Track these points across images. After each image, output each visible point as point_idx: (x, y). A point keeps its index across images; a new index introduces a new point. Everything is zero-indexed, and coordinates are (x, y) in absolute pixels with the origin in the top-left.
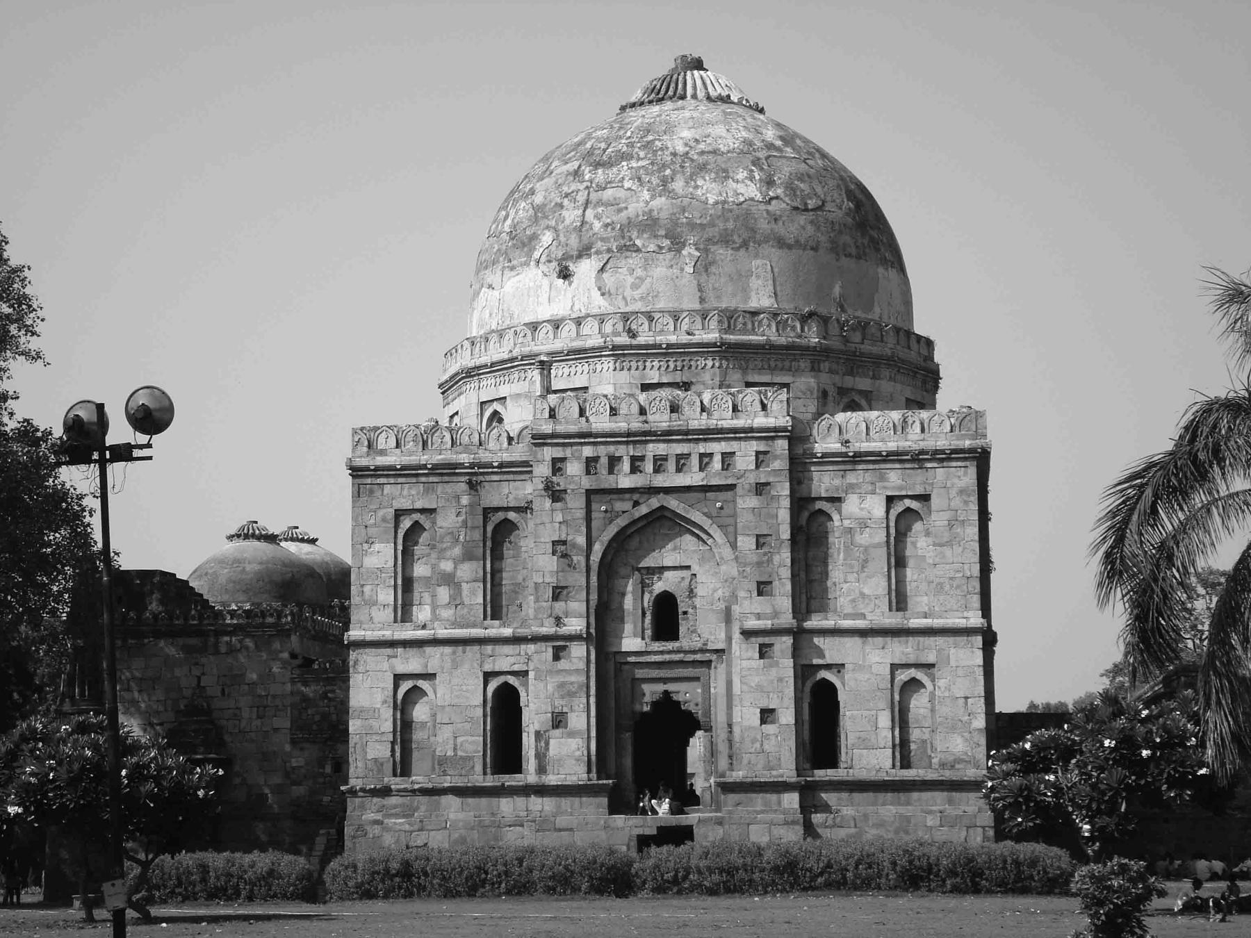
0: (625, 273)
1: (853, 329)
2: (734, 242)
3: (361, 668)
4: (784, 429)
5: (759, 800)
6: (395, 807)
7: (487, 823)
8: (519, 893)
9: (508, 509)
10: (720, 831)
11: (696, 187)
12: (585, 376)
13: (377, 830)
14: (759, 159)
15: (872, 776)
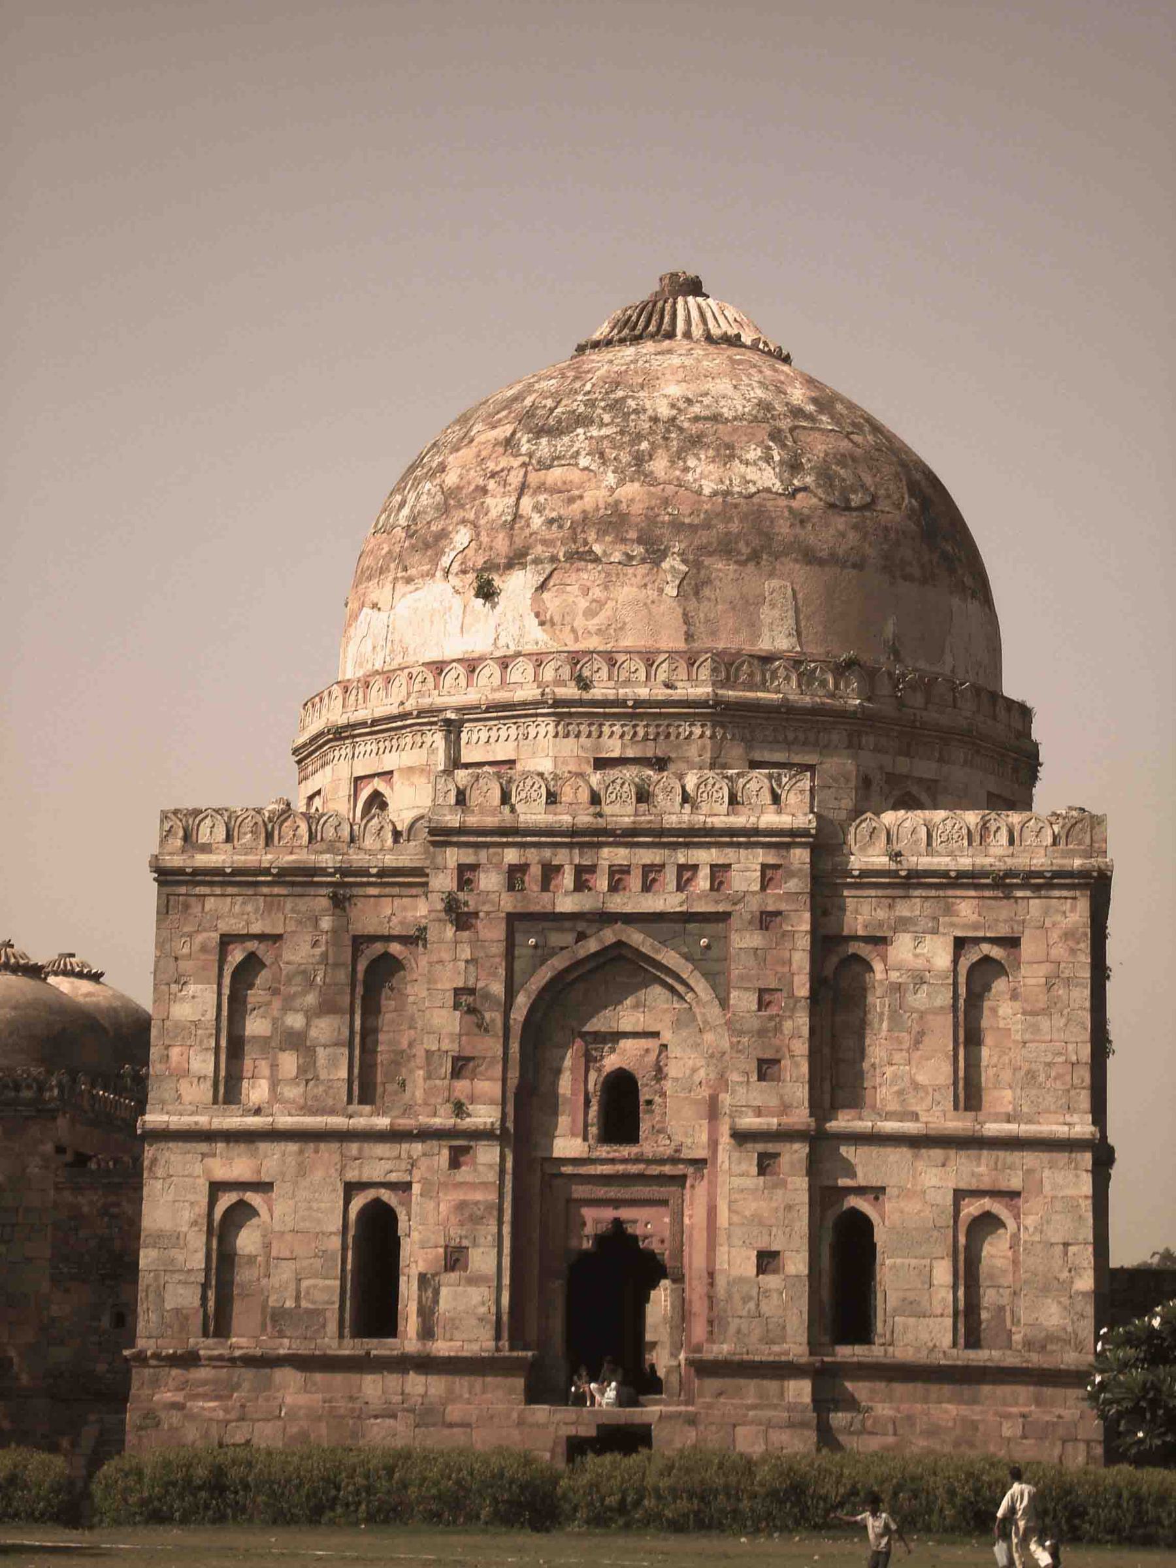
0: (576, 592)
1: (913, 687)
2: (739, 553)
3: (160, 1172)
4: (805, 833)
5: (751, 1388)
6: (205, 1383)
7: (342, 1411)
8: (386, 1521)
10: (691, 1435)
11: (686, 469)
12: (511, 744)
13: (175, 1418)
14: (780, 431)
15: (923, 1358)
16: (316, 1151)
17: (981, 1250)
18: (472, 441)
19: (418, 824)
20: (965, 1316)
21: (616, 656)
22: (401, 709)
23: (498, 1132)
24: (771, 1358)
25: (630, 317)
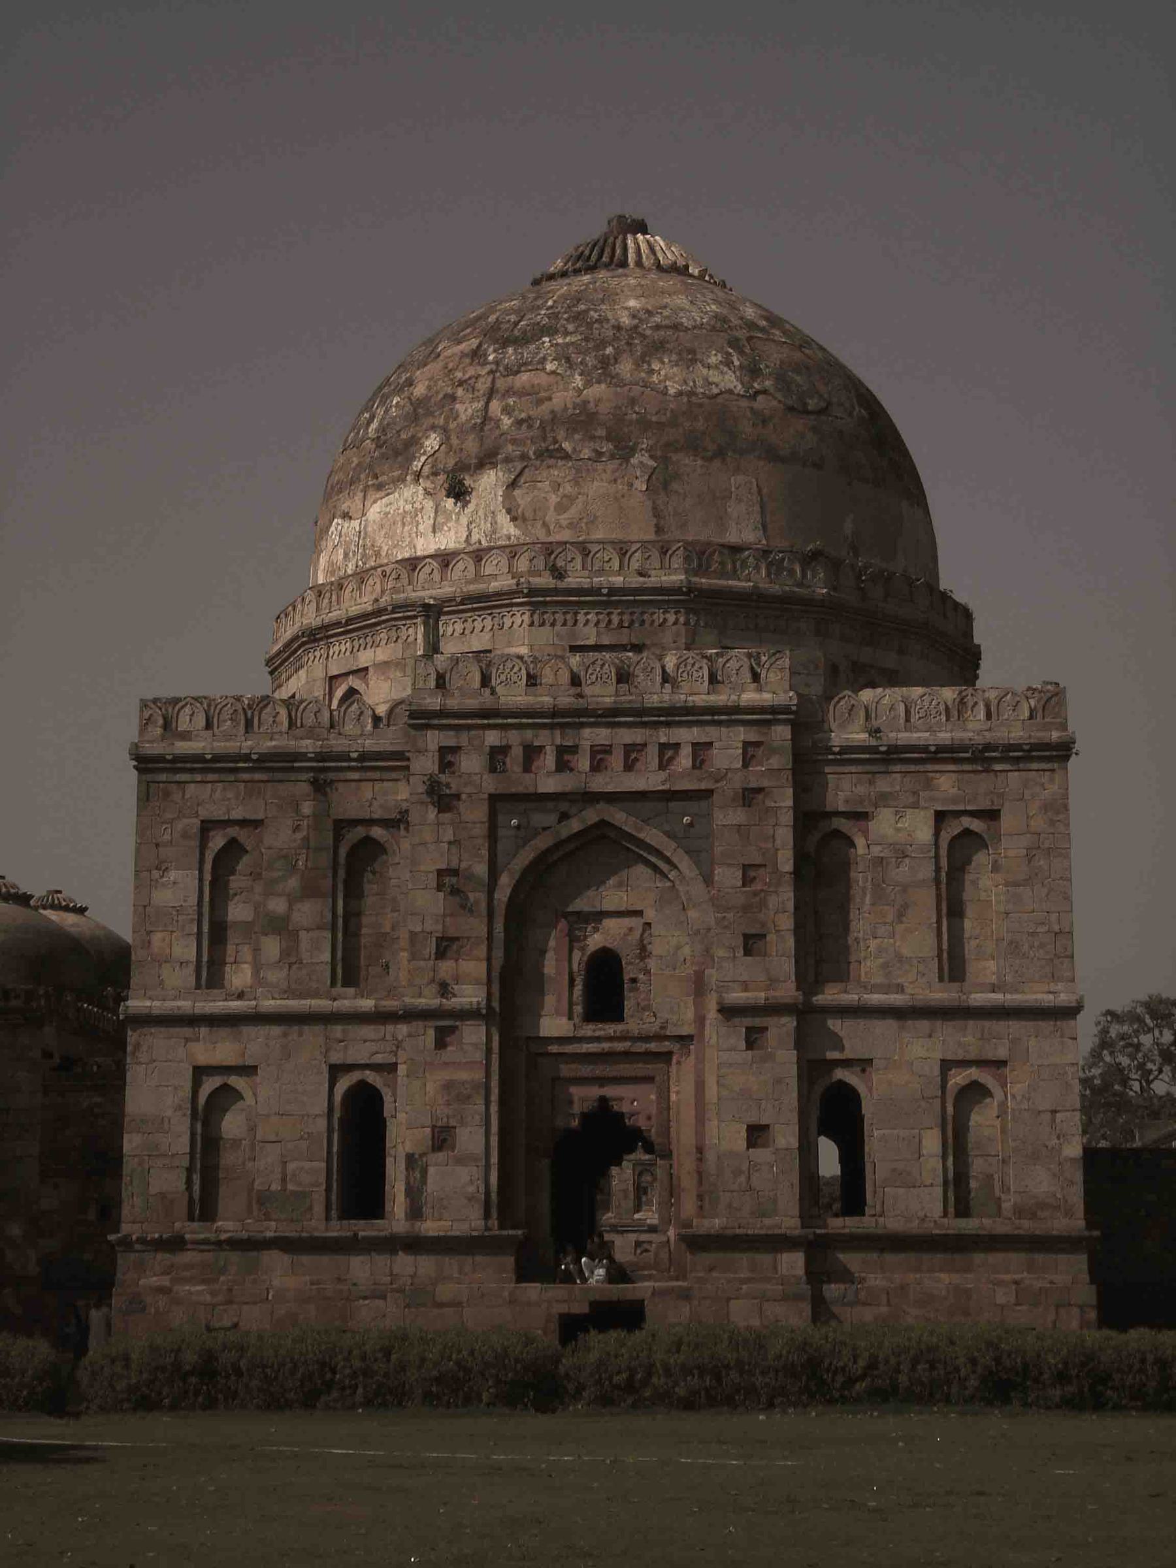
0: (548, 487)
2: (705, 449)
3: (143, 1057)
4: (786, 710)
5: (743, 1259)
8: (384, 1405)
9: (371, 822)
10: (686, 1309)
11: (652, 372)
12: (487, 636)
13: (162, 1301)
14: (737, 340)
15: (914, 1227)
16: (300, 1034)
17: (969, 1120)
18: (439, 355)
19: (397, 710)
20: (955, 1185)
21: (588, 545)
22: (375, 607)
23: (484, 1011)
24: (763, 1232)
25: (582, 253)
